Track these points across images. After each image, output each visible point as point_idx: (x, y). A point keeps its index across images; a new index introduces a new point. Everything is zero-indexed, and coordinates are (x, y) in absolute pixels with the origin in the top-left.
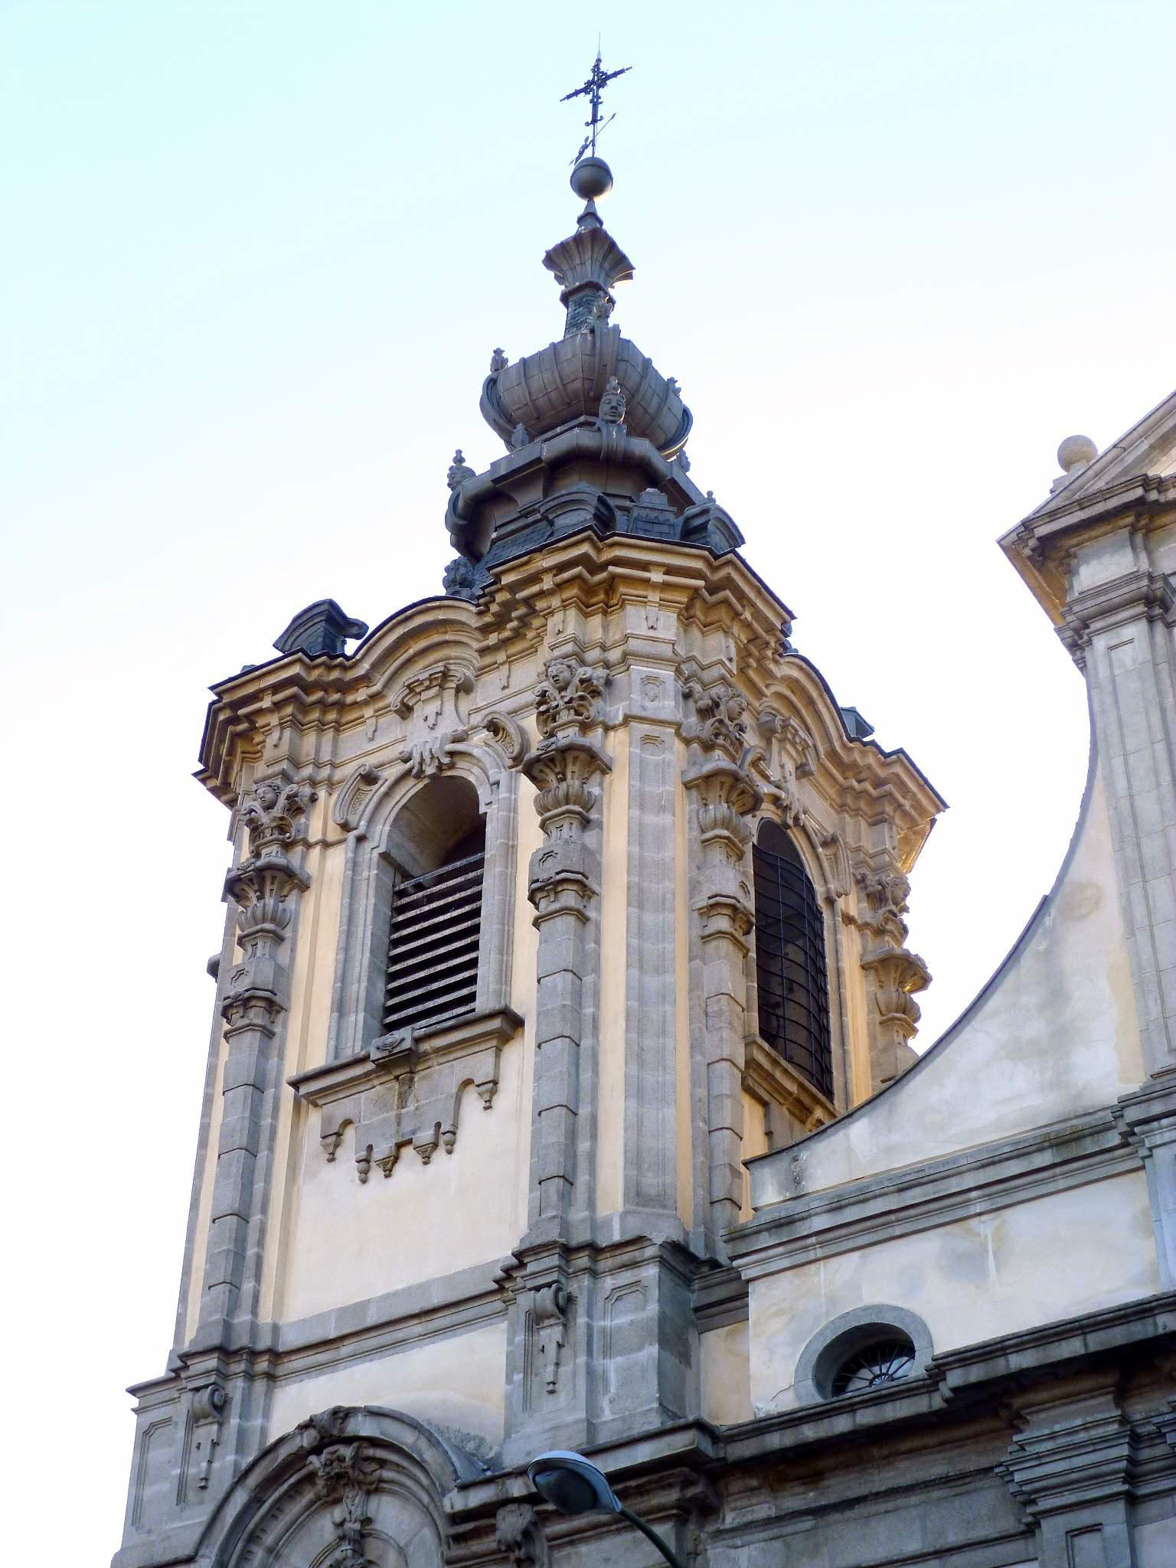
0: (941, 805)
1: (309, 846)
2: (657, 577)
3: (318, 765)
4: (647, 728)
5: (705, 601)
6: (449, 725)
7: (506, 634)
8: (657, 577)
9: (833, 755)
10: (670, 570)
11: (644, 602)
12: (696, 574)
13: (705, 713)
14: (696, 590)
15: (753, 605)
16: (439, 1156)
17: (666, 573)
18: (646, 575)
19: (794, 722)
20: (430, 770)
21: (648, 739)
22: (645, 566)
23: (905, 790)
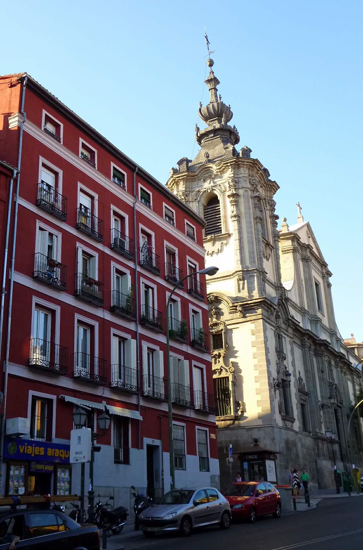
0: (279, 187)
1: (190, 202)
2: (246, 164)
3: (189, 188)
4: (246, 189)
5: (252, 166)
6: (212, 184)
7: (220, 170)
8: (246, 164)
9: (265, 183)
10: (247, 162)
11: (243, 167)
12: (251, 163)
13: (253, 185)
14: (251, 165)
15: (258, 166)
16: (219, 254)
17: (247, 163)
18: (244, 163)
19: (261, 181)
20: (209, 191)
21: (246, 191)
22: (244, 162)
23: (274, 186)
